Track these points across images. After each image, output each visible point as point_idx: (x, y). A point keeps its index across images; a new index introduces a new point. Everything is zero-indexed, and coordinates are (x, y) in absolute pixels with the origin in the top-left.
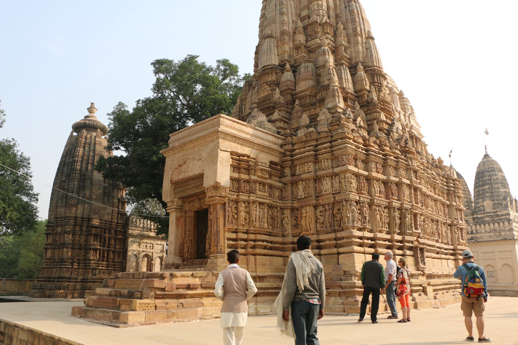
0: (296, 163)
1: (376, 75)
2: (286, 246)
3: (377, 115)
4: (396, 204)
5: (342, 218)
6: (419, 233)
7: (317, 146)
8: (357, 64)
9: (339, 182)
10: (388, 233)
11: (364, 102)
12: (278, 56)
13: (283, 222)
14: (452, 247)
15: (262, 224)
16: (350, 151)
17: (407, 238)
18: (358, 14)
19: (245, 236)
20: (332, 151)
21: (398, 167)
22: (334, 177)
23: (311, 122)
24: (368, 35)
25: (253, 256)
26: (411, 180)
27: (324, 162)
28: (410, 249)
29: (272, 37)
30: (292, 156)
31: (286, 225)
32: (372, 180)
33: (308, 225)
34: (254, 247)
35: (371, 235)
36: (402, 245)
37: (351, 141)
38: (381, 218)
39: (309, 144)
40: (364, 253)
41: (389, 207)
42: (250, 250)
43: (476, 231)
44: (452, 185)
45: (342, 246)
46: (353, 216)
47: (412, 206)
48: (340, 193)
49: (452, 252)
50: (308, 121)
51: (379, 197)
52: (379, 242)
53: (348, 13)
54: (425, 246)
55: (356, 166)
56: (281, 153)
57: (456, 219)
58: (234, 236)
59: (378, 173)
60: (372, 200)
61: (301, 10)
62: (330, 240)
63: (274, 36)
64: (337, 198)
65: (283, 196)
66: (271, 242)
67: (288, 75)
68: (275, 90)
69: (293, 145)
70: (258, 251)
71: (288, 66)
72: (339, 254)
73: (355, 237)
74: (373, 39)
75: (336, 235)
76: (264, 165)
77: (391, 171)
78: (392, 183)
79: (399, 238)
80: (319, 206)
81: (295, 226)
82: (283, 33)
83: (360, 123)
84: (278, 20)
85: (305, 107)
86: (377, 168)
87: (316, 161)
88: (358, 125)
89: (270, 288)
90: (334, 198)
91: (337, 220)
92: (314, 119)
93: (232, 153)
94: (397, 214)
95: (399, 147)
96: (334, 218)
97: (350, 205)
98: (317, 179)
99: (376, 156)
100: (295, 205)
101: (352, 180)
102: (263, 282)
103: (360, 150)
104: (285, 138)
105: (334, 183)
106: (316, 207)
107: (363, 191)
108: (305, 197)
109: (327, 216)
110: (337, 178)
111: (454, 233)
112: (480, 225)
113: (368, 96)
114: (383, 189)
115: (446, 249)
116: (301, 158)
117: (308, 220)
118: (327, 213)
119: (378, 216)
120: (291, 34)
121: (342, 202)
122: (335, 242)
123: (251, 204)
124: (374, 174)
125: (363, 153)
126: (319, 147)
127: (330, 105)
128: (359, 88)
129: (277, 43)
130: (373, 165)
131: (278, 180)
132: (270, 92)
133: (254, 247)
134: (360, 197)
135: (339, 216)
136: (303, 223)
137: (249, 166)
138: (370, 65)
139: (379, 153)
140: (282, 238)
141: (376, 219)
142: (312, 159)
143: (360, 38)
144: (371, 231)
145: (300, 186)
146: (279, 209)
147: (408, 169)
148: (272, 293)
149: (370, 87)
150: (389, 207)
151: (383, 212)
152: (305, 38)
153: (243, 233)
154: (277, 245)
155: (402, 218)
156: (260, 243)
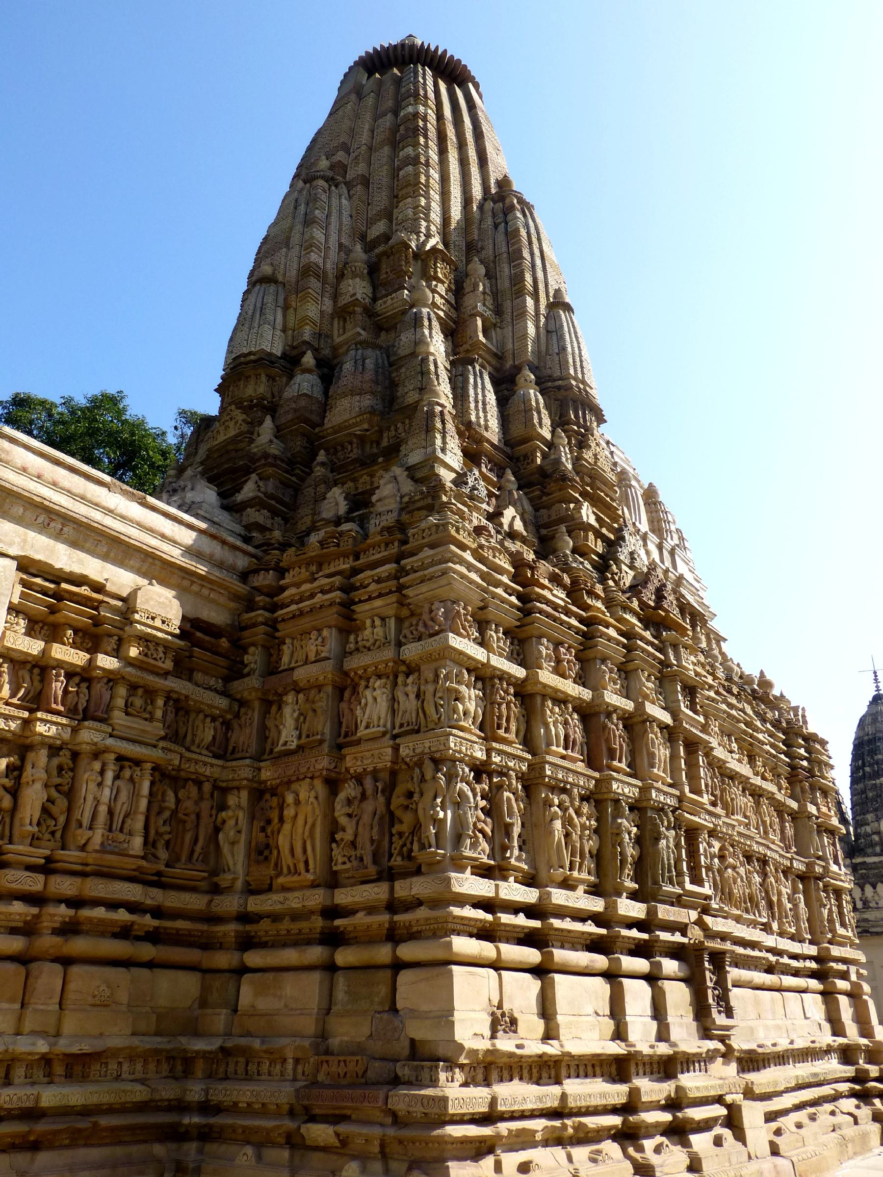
0: (284, 629)
1: (574, 407)
2: (220, 929)
3: (568, 509)
4: (625, 788)
5: (417, 828)
6: (707, 898)
7: (355, 571)
8: (518, 369)
9: (418, 696)
10: (595, 890)
11: (532, 474)
12: (284, 331)
13: (221, 836)
14: (813, 950)
15: (121, 837)
16: (460, 586)
17: (665, 912)
18: (530, 243)
19: (35, 883)
20: (400, 588)
21: (631, 666)
22: (400, 679)
23: (351, 511)
24: (555, 297)
25: (58, 968)
26: (675, 714)
27: (373, 626)
28: (676, 952)
29: (276, 282)
30: (273, 608)
31: (226, 849)
32: (539, 700)
33: (298, 850)
34: (69, 929)
35: (530, 896)
36: (645, 936)
37: (468, 556)
38: (567, 835)
39: (332, 570)
40: (497, 966)
41: (598, 798)
42: (48, 942)
43: (865, 903)
44: (802, 751)
45: (413, 936)
46: (460, 822)
47: (680, 799)
48: (418, 731)
49: (813, 965)
50: (343, 508)
51: (563, 757)
52: (556, 923)
53: (501, 237)
54: (728, 946)
55: (482, 643)
56: (235, 597)
57: (819, 858)
59: (563, 676)
60: (536, 768)
61: (370, 223)
62: (371, 910)
63: (280, 278)
64: (404, 752)
66: (158, 912)
67: (305, 383)
68: (261, 423)
69: (282, 572)
70: (79, 945)
71: (309, 359)
72: (398, 966)
73: (462, 900)
74: (568, 308)
75: (392, 890)
76: (158, 623)
77: (608, 673)
78: (609, 715)
79: (635, 910)
80: (345, 781)
81: (260, 853)
82: (306, 271)
83: (511, 525)
84: (296, 238)
85: (339, 471)
86: (558, 661)
87: (348, 624)
88: (506, 527)
89: (110, 1110)
90: (396, 749)
91: (401, 835)
92: (360, 503)
93: (25, 565)
94: (628, 827)
95: (635, 604)
96: (392, 825)
97: (451, 778)
98: (346, 687)
99: (555, 619)
100: (265, 775)
101: (463, 689)
102: (84, 1078)
103: (500, 591)
104: (260, 554)
105: (401, 698)
106: (333, 785)
107: (501, 732)
108: (300, 748)
109: (366, 818)
110: (410, 680)
111: (816, 905)
112: (874, 887)
113: (545, 456)
114: (577, 734)
115: (795, 957)
116: (302, 613)
117: (300, 830)
118: (369, 807)
119: (558, 824)
120: (331, 276)
121: (420, 764)
122: (384, 918)
123: (83, 762)
124: (546, 676)
125: (512, 605)
126: (361, 576)
127: (415, 458)
128: (517, 430)
129: (285, 299)
130: (545, 649)
131: (220, 685)
132: (245, 427)
133: (69, 929)
134: (488, 752)
135: (408, 818)
136: (283, 841)
137: (97, 622)
138: (557, 374)
139: (568, 613)
140: (205, 898)
141: (551, 833)
142: (332, 616)
143: (530, 302)
144: (530, 881)
145: (287, 711)
146: (207, 787)
147: (666, 677)
148: (113, 1129)
149: (553, 432)
150: (598, 798)
151: (578, 813)
152: (369, 291)
153: (30, 868)
154: (180, 924)
155: (647, 840)
156: (100, 912)
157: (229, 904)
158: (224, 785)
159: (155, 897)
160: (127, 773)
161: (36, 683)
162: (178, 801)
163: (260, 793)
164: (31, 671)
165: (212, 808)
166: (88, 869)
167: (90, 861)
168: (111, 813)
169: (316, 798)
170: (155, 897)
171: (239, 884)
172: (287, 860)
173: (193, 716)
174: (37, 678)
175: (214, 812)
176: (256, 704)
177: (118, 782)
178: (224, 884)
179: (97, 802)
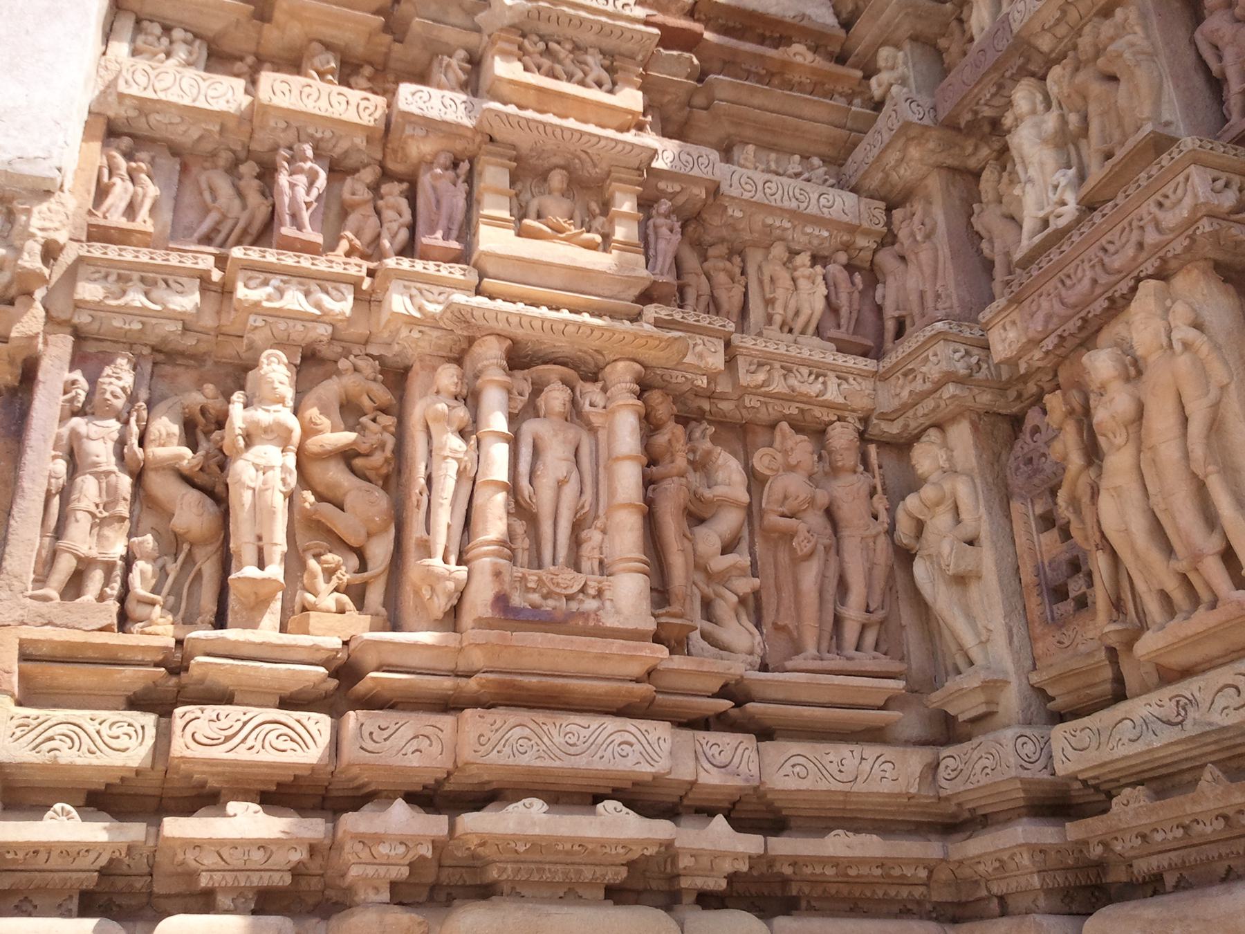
15: (571, 581)
19: (303, 742)
31: (941, 598)
33: (1184, 519)
58: (119, 742)
65: (890, 312)
66: (757, 813)
81: (1059, 594)
100: (1006, 339)
117: (1169, 452)
136: (1120, 514)
140: (916, 760)
146: (842, 437)
154: (838, 844)
157: (995, 763)
158: (894, 429)
159: (724, 762)
160: (556, 397)
161: (254, 198)
162: (755, 480)
163: (1007, 426)
164: (232, 169)
165: (873, 492)
166: (472, 684)
167: (477, 659)
168: (521, 509)
169: (1198, 326)
170: (724, 762)
171: (1012, 700)
172: (1152, 574)
173: (754, 257)
174: (251, 186)
175: (880, 503)
176: (935, 183)
177: (530, 428)
178: (965, 709)
179: (470, 481)
